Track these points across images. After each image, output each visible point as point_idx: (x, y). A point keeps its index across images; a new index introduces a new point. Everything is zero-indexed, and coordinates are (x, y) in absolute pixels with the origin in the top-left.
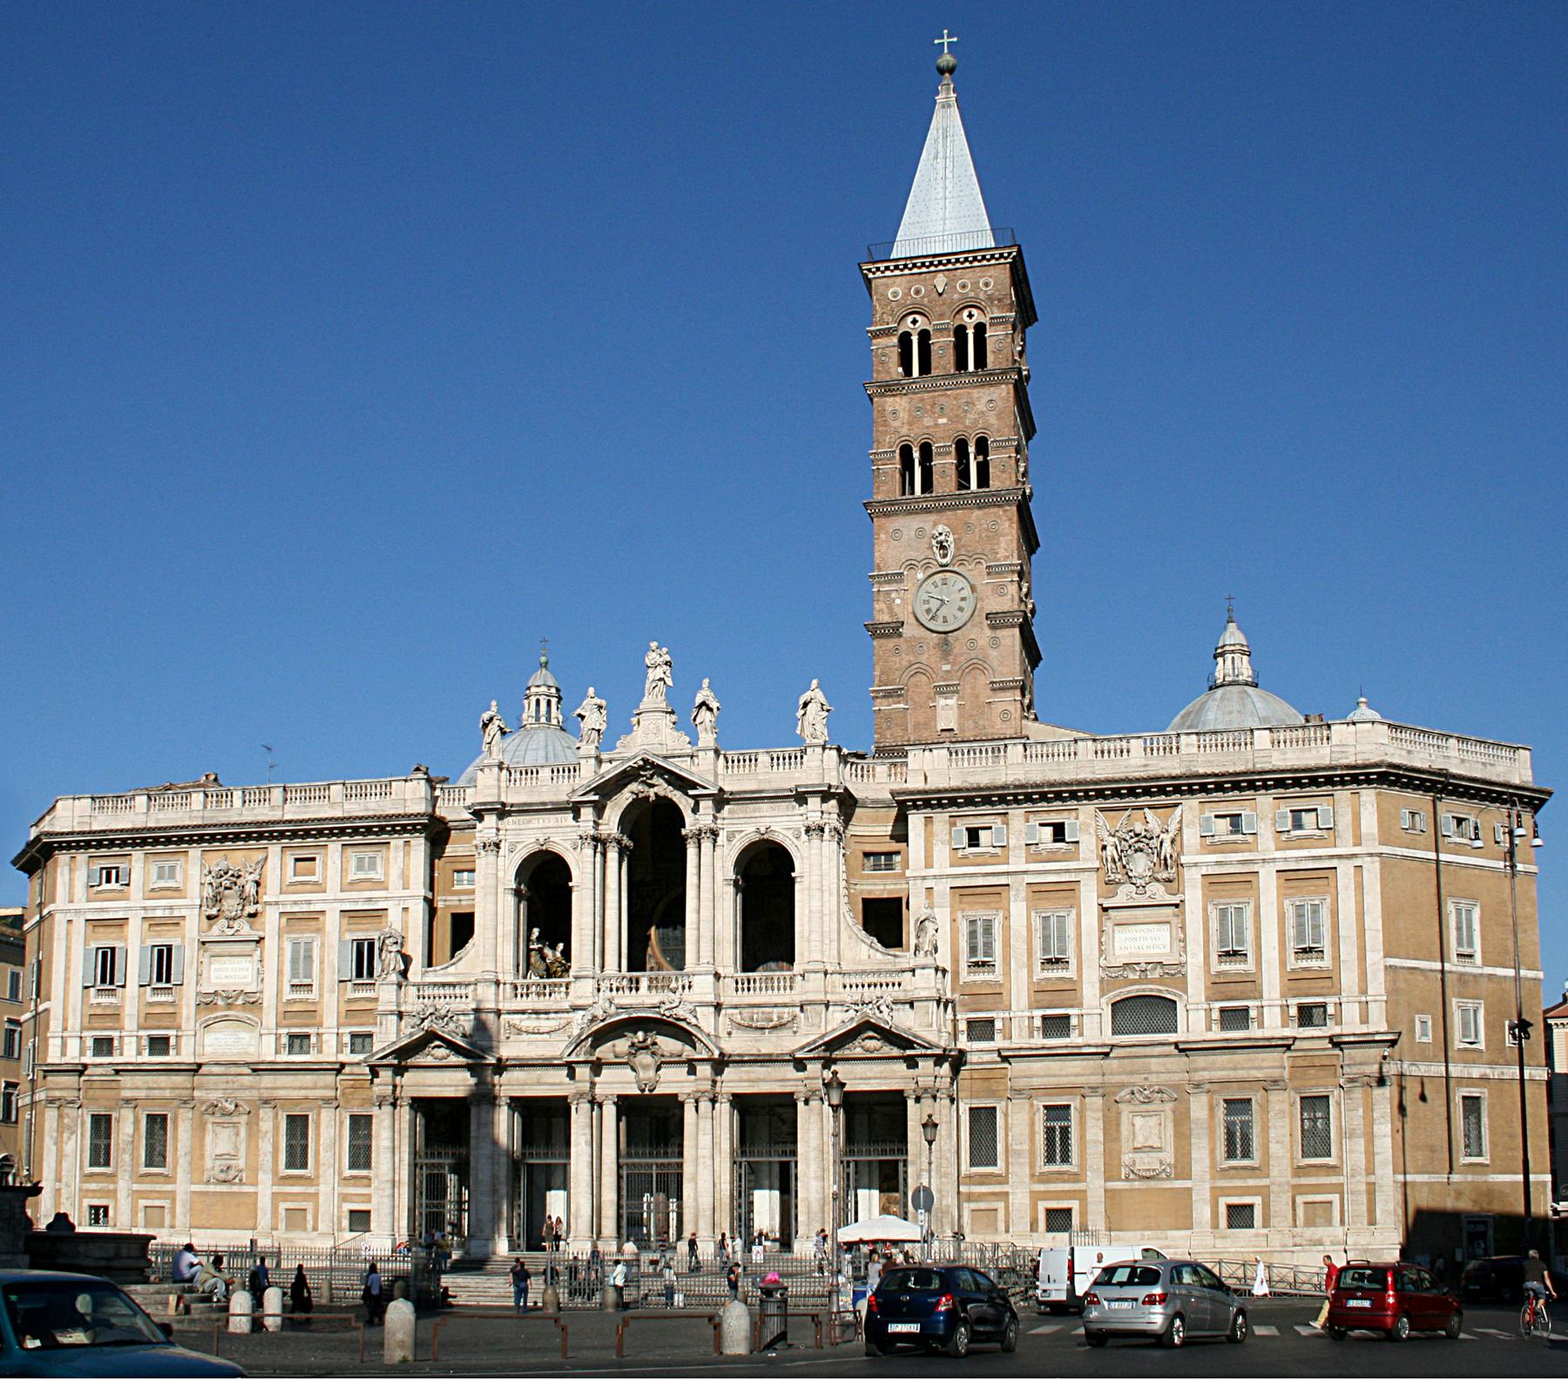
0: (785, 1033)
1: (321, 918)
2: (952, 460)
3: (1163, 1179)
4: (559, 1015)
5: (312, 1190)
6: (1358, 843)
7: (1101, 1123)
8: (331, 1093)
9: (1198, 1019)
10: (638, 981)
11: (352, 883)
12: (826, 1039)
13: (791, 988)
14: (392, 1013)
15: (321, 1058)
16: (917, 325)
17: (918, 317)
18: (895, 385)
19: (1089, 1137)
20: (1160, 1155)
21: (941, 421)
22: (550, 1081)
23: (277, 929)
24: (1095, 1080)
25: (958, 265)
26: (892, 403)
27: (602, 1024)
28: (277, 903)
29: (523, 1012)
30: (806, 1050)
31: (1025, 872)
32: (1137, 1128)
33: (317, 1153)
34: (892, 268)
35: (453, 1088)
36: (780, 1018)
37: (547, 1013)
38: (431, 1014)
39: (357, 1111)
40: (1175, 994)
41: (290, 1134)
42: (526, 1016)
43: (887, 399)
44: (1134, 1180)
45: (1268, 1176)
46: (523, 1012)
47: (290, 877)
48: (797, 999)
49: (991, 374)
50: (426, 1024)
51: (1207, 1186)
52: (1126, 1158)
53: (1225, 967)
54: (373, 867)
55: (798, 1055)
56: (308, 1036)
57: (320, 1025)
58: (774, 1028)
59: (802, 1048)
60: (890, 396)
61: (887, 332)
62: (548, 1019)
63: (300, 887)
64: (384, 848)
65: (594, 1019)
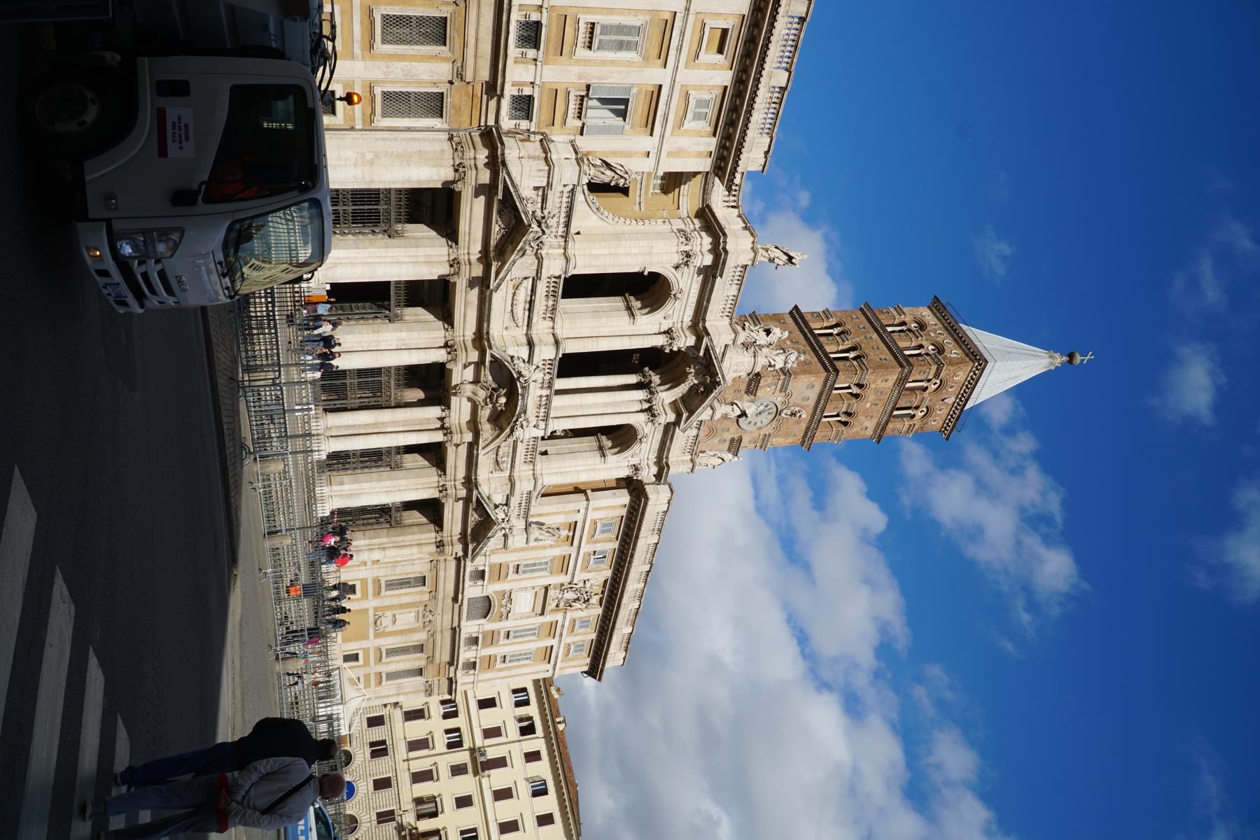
1: (661, 61)
2: (844, 410)
3: (375, 628)
5: (357, 50)
6: (561, 669)
7: (412, 601)
8: (469, 77)
9: (475, 629)
11: (687, 95)
14: (549, 185)
15: (510, 61)
16: (932, 385)
17: (937, 386)
18: (903, 383)
19: (403, 598)
20: (390, 625)
21: (868, 405)
22: (468, 312)
23: (658, 8)
24: (440, 596)
26: (893, 378)
27: (515, 376)
28: (687, 9)
30: (479, 496)
31: (578, 553)
32: (409, 614)
33: (401, 58)
35: (467, 230)
36: (503, 462)
37: (530, 310)
38: (544, 233)
39: (448, 101)
40: (490, 618)
41: (421, 20)
42: (529, 292)
43: (897, 376)
44: (374, 618)
45: (375, 665)
47: (711, 23)
48: (516, 475)
50: (535, 226)
51: (370, 645)
52: (389, 613)
53: (502, 634)
54: (697, 117)
56: (536, 46)
57: (546, 62)
58: (497, 461)
59: (480, 494)
61: (937, 375)
62: (524, 310)
63: (698, 35)
64: (710, 129)
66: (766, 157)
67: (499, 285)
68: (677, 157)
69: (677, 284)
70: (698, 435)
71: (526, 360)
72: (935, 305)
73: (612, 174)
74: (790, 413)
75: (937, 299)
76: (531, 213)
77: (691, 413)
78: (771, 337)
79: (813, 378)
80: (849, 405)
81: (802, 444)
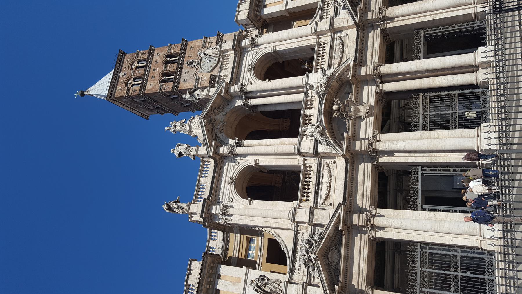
0: (346, 40)
2: (169, 65)
4: (322, 169)
10: (307, 116)
12: (350, 8)
13: (325, 44)
17: (129, 82)
25: (120, 69)
26: (148, 87)
29: (317, 193)
30: (355, 17)
34: (112, 90)
46: (317, 193)
49: (150, 54)
50: (313, 257)
55: (357, 20)
59: (354, 19)
60: (146, 88)
61: (128, 90)
62: (323, 177)
65: (322, 133)
66: (190, 270)
67: (337, 209)
68: (236, 277)
69: (232, 190)
70: (220, 71)
71: (319, 144)
72: (147, 116)
73: (265, 289)
74: (194, 63)
75: (147, 119)
76: (316, 269)
77: (220, 94)
78: (178, 151)
79: (184, 86)
80: (167, 68)
81: (187, 42)
